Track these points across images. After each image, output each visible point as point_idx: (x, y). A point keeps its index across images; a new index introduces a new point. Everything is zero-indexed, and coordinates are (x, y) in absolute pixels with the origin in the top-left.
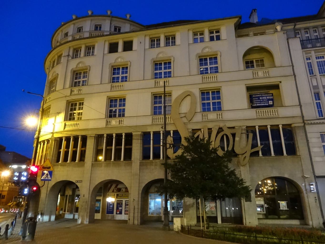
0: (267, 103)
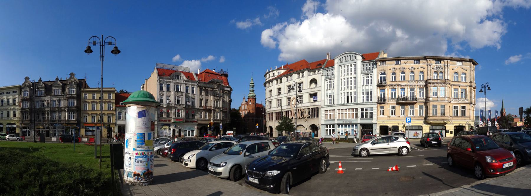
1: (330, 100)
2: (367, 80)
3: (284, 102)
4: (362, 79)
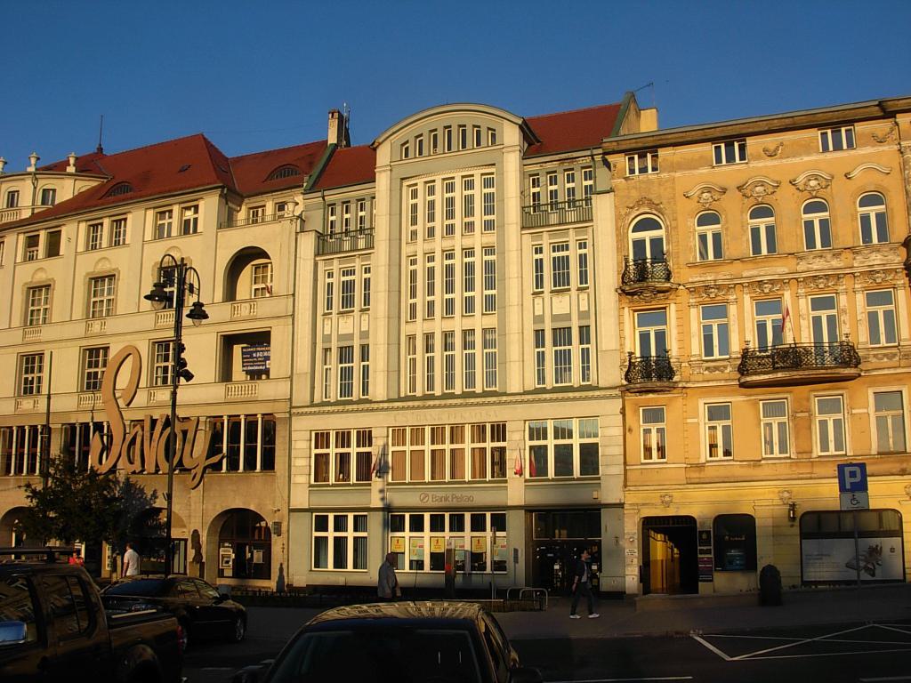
0: (263, 365)
1: (346, 374)
2: (561, 264)
3: (64, 373)
4: (530, 258)
